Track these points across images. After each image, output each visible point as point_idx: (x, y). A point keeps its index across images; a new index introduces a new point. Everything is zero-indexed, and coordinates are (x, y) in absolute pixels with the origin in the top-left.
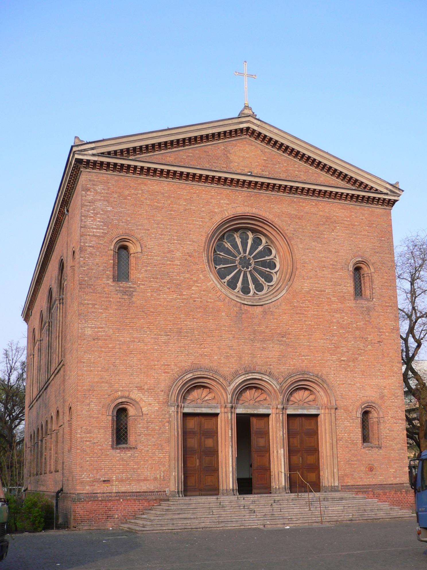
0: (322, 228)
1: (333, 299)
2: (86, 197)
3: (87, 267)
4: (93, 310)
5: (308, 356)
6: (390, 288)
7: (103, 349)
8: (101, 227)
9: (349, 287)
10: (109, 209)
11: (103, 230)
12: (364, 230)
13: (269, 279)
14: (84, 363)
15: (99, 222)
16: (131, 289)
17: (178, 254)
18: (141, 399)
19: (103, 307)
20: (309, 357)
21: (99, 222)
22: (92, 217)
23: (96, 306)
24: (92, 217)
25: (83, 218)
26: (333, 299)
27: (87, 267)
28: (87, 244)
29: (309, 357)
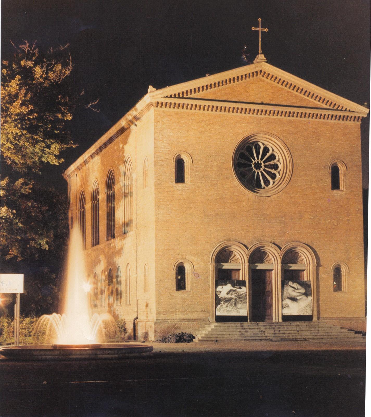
0: (311, 140)
1: (317, 191)
2: (157, 126)
3: (159, 174)
4: (163, 203)
5: (299, 230)
6: (357, 181)
7: (170, 228)
8: (167, 147)
9: (328, 181)
10: (171, 134)
11: (168, 148)
12: (340, 140)
13: (273, 176)
14: (158, 237)
15: (165, 143)
16: (186, 188)
17: (215, 163)
18: (193, 260)
19: (169, 201)
20: (299, 232)
21: (165, 143)
22: (161, 140)
23: (165, 200)
24: (161, 140)
25: (156, 141)
26: (317, 191)
27: (159, 174)
28: (158, 159)
29: (299, 232)
